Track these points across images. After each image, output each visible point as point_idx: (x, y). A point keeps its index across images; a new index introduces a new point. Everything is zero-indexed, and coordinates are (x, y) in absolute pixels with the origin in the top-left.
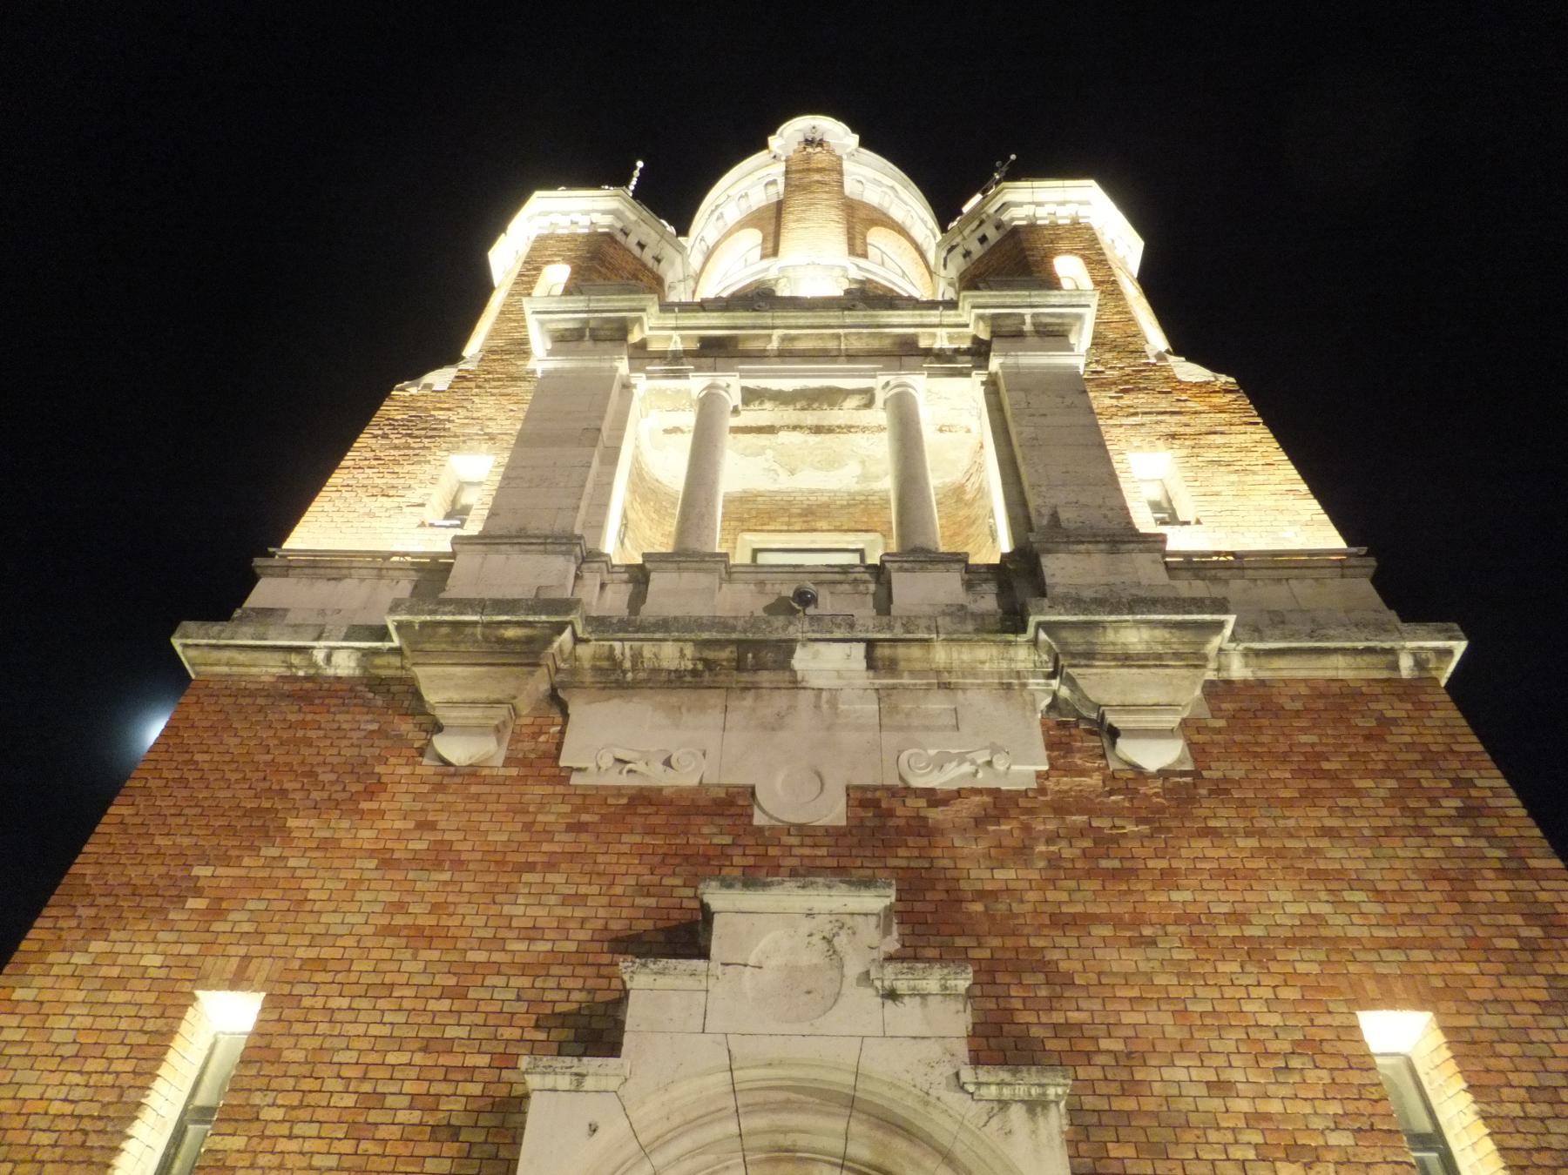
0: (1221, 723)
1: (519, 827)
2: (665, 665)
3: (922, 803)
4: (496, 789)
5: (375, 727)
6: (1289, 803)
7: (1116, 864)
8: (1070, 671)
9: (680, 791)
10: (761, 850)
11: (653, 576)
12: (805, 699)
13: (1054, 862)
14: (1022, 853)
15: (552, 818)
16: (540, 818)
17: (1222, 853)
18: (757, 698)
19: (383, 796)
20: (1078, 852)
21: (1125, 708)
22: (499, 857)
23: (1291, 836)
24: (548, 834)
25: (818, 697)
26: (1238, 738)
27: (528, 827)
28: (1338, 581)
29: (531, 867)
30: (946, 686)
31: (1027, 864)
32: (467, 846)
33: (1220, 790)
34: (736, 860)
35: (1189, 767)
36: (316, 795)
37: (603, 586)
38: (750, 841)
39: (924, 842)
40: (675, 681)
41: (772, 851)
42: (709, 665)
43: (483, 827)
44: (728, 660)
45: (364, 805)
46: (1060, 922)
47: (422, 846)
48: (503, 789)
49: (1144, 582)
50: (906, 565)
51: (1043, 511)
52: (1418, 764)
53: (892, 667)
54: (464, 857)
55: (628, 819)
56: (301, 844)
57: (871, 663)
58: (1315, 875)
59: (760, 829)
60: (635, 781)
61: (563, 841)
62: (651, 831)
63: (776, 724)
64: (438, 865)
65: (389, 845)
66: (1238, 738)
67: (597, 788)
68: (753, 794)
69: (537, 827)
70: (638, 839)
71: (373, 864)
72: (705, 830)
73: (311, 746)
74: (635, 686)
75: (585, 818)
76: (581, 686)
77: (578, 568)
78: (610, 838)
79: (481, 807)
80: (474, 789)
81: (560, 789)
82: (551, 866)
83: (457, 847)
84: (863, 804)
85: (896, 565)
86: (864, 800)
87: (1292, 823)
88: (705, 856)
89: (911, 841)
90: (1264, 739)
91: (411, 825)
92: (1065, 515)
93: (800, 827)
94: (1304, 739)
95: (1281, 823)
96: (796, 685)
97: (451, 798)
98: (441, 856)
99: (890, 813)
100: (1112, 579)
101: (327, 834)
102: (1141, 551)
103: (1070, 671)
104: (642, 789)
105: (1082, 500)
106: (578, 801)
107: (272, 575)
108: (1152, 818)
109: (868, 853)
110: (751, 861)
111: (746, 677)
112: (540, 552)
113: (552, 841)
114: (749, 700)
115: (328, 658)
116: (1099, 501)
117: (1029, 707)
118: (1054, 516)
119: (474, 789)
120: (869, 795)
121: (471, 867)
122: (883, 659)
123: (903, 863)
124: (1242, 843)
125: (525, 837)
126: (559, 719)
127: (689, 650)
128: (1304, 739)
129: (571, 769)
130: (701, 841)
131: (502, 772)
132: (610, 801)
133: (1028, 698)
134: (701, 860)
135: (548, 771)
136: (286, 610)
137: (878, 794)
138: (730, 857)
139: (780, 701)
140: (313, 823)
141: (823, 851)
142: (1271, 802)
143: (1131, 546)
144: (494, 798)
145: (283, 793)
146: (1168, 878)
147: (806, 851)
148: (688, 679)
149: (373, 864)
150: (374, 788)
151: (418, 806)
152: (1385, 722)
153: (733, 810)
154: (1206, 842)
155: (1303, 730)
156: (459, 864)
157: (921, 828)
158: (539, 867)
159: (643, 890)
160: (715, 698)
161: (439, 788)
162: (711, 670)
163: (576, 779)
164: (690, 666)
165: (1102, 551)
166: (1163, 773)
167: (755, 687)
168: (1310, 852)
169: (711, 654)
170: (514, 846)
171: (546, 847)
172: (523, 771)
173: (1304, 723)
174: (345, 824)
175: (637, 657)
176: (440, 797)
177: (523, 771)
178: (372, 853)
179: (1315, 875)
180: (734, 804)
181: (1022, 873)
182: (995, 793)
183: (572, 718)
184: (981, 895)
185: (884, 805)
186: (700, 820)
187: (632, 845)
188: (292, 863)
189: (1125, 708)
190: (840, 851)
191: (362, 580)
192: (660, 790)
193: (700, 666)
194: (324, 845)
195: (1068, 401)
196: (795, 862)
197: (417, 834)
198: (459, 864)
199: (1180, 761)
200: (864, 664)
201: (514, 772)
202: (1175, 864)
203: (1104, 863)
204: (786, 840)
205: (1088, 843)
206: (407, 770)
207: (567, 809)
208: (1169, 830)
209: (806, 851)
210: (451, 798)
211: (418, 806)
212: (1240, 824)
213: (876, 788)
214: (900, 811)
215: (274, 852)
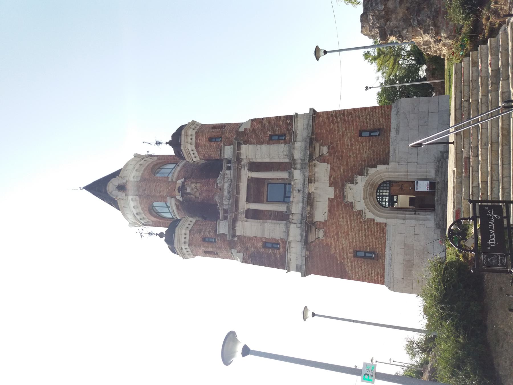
6: (334, 136)
14: (339, 168)
21: (320, 152)
24: (334, 222)
30: (314, 174)
33: (331, 143)
46: (347, 165)
52: (329, 119)
53: (311, 180)
58: (343, 136)
61: (335, 220)
62: (334, 210)
63: (320, 195)
74: (312, 213)
82: (339, 221)
86: (331, 185)
92: (285, 154)
96: (313, 193)
98: (337, 234)
108: (335, 152)
139: (316, 195)
145: (328, 256)
146: (343, 152)
150: (327, 244)
152: (323, 121)
156: (338, 232)
157: (335, 178)
159: (342, 210)
160: (315, 203)
161: (327, 236)
163: (326, 219)
166: (329, 149)
167: (313, 198)
175: (309, 213)
179: (343, 136)
180: (331, 200)
184: (344, 173)
189: (320, 152)
194: (335, 248)
198: (338, 232)
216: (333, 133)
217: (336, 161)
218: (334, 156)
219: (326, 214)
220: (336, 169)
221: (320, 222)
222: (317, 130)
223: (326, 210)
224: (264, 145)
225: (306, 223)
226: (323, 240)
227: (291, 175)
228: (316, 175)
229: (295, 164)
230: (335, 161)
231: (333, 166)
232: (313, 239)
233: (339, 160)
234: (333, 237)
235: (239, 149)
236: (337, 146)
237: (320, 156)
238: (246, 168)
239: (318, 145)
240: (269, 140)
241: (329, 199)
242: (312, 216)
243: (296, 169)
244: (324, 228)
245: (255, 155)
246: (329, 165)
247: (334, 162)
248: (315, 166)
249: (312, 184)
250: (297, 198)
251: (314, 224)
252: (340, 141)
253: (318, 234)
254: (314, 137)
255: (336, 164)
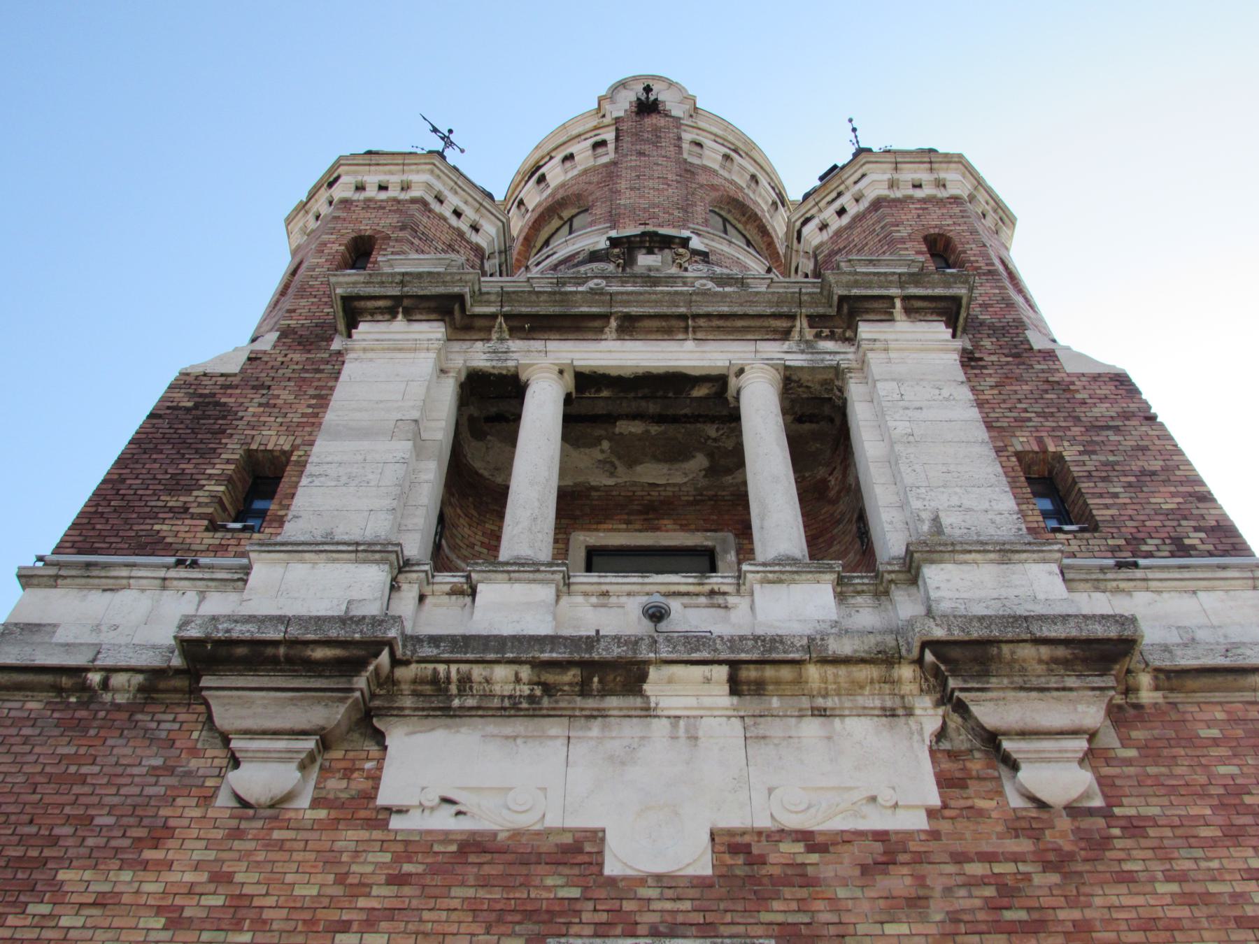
0: (1132, 753)
1: (331, 878)
2: (497, 689)
3: (800, 847)
4: (303, 835)
5: (158, 762)
6: (1213, 843)
7: (1022, 915)
8: (962, 695)
9: (516, 834)
10: (615, 905)
11: (480, 587)
12: (660, 727)
13: (954, 918)
14: (916, 903)
15: (369, 869)
16: (355, 868)
17: (1139, 900)
18: (603, 728)
19: (170, 843)
20: (978, 903)
21: (1024, 734)
22: (307, 915)
23: (1214, 880)
24: (363, 888)
25: (675, 726)
26: (1152, 770)
27: (341, 879)
28: (1251, 593)
29: (345, 927)
30: (820, 713)
31: (924, 919)
32: (270, 901)
33: (1134, 827)
34: (586, 917)
35: (1098, 802)
36: (90, 842)
37: (422, 598)
38: (602, 893)
39: (803, 893)
40: (511, 708)
41: (628, 906)
42: (548, 689)
43: (289, 878)
44: (570, 684)
45: (148, 854)
47: (218, 901)
48: (316, 835)
49: (1041, 596)
50: (770, 576)
51: (924, 515)
53: (759, 688)
54: (267, 914)
55: (459, 869)
56: (75, 898)
57: (735, 687)
59: (612, 881)
60: (465, 824)
62: (484, 883)
64: (237, 926)
65: (179, 901)
66: (1152, 770)
67: (421, 832)
68: (603, 840)
69: (351, 880)
70: (470, 892)
71: (160, 922)
72: (549, 882)
73: (84, 783)
75: (407, 868)
76: (400, 713)
77: (394, 579)
78: (437, 891)
79: (286, 856)
80: (276, 835)
81: (377, 835)
83: (256, 902)
84: (734, 849)
85: (759, 576)
87: (1215, 864)
88: (548, 911)
89: (787, 892)
90: (1178, 771)
91: (204, 877)
92: (946, 520)
93: (658, 877)
94: (1222, 770)
95: (1203, 864)
96: (648, 712)
97: (250, 845)
99: (762, 861)
100: (1004, 593)
101: (106, 888)
102: (1035, 561)
103: (962, 695)
104: (473, 833)
105: (967, 503)
106: (400, 847)
107: (38, 586)
108: (1056, 862)
109: (740, 908)
110: (603, 917)
111: (591, 703)
112: (349, 561)
113: (368, 895)
114: (595, 729)
115: (105, 685)
116: (986, 505)
117: (916, 737)
118: (936, 520)
119: (276, 835)
120: (739, 839)
121: (275, 926)
122: (749, 683)
123: (780, 918)
124: (1162, 888)
125: (338, 891)
126: (374, 750)
127: (525, 673)
128: (1222, 770)
129: (389, 810)
130: (545, 895)
131: (310, 814)
132: (436, 848)
133: (914, 727)
134: (546, 917)
135: (363, 814)
136: (55, 626)
137: (747, 839)
138: (578, 913)
139: (630, 730)
140: (88, 875)
141: (687, 905)
142: (1190, 841)
143: (1024, 556)
144: (302, 845)
145: (54, 841)
147: (669, 906)
148: (525, 705)
149: (160, 922)
150: (160, 835)
151: (211, 855)
153: (580, 858)
154: (1123, 889)
155: (1223, 761)
157: (800, 877)
158: (355, 927)
160: (556, 728)
161: (237, 834)
162: (550, 696)
164: (527, 692)
165: (992, 561)
166: (1073, 810)
168: (1238, 898)
169: (550, 677)
170: (326, 902)
171: (362, 903)
172: (334, 814)
173: (1223, 751)
174: (126, 876)
175: (465, 681)
176: (237, 844)
177: (334, 814)
178: (159, 910)
180: (580, 851)
181: (919, 928)
182: (881, 836)
183: (391, 751)
185: (755, 851)
186: (541, 869)
187: (464, 899)
188: (64, 922)
189: (1024, 734)
190: (705, 904)
191: (143, 590)
192: (495, 834)
193: (538, 692)
195: (945, 393)
196: (654, 918)
197: (212, 887)
199: (1086, 795)
200: (726, 688)
201: (322, 814)
202: (1089, 913)
203: (1008, 915)
204: (644, 892)
205: (990, 892)
206: (197, 813)
207: (387, 857)
208: (1080, 874)
209: (669, 906)
210: (250, 845)
211: (211, 855)
212: (1157, 867)
213: (744, 833)
214: (773, 858)
215: (45, 909)
216: (1234, 835)
217: (982, 882)
218: (1016, 858)
219: (444, 821)
220: (899, 882)
221: (375, 778)
222: (1209, 715)
223: (489, 816)
224: (974, 413)
225: (375, 647)
226: (207, 799)
227: (783, 571)
228: (812, 728)
229: (881, 593)
230: (976, 869)
231: (920, 858)
232: (225, 717)
233: (993, 907)
234: (221, 878)
235: (916, 308)
236: (1127, 878)
237: (991, 739)
238: (798, 360)
239: (1091, 713)
240: (1019, 455)
241: (597, 836)
242: (441, 702)
243: (841, 597)
244: (316, 803)
245: (900, 381)
246: (919, 822)
247: (960, 858)
248: (891, 713)
249: (721, 698)
250: (608, 611)
251: (368, 725)
252: (1188, 900)
253: (265, 757)
254: (1147, 695)
255: (940, 875)
